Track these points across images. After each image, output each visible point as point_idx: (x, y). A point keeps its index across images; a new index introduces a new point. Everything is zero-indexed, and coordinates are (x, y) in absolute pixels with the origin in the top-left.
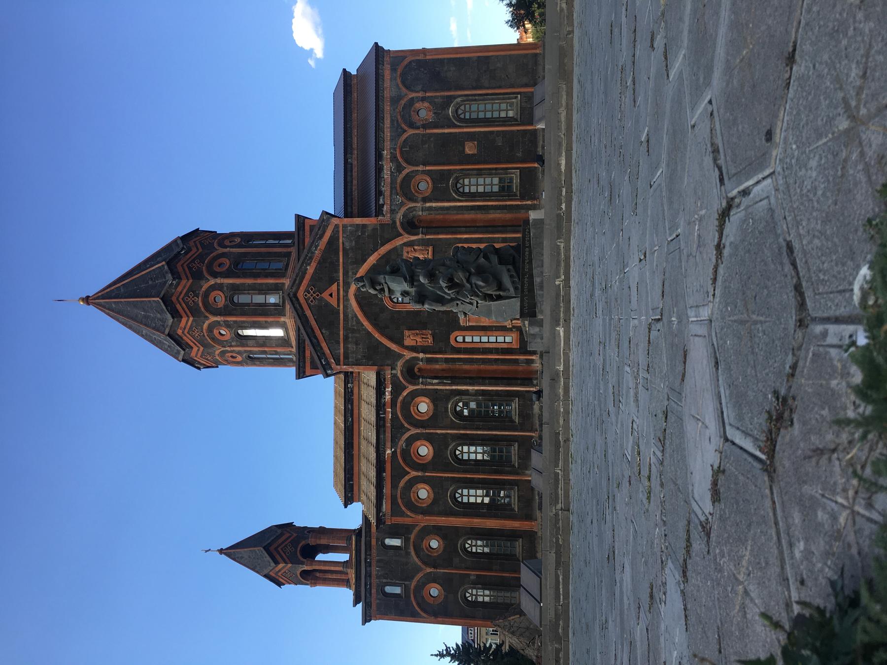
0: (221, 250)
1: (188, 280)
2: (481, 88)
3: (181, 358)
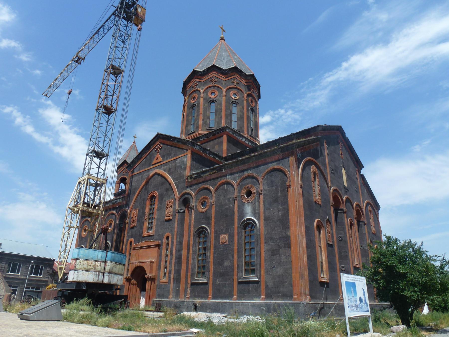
0: (224, 90)
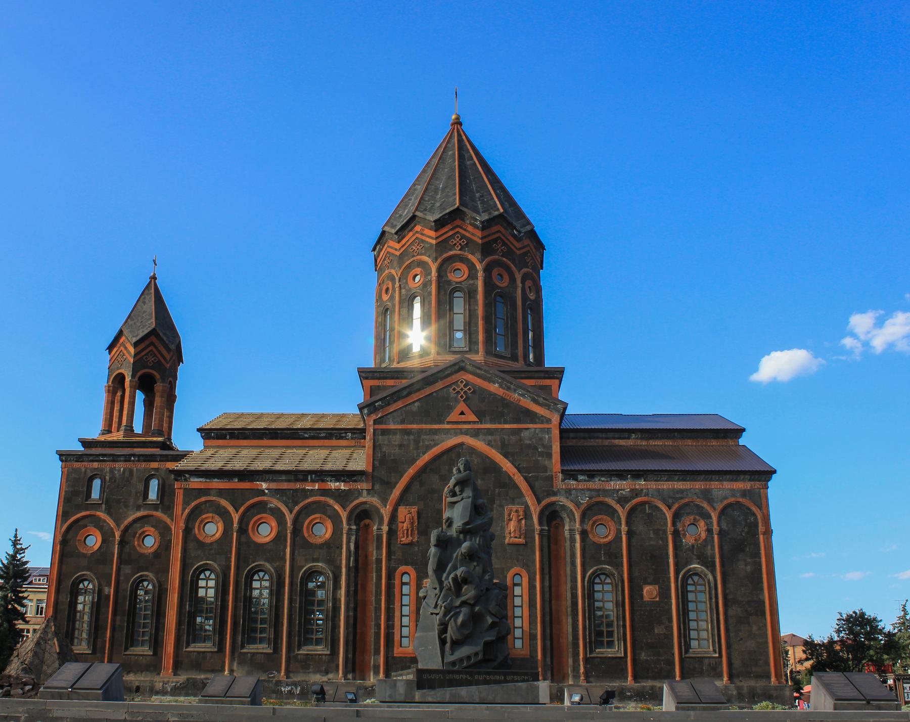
0: (519, 277)
1: (482, 239)
3: (387, 229)
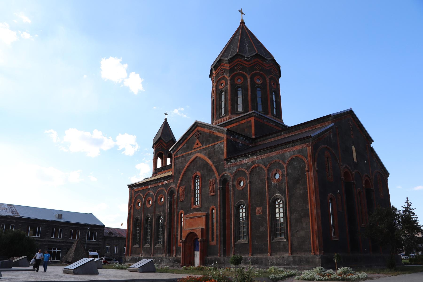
2: (291, 213)
